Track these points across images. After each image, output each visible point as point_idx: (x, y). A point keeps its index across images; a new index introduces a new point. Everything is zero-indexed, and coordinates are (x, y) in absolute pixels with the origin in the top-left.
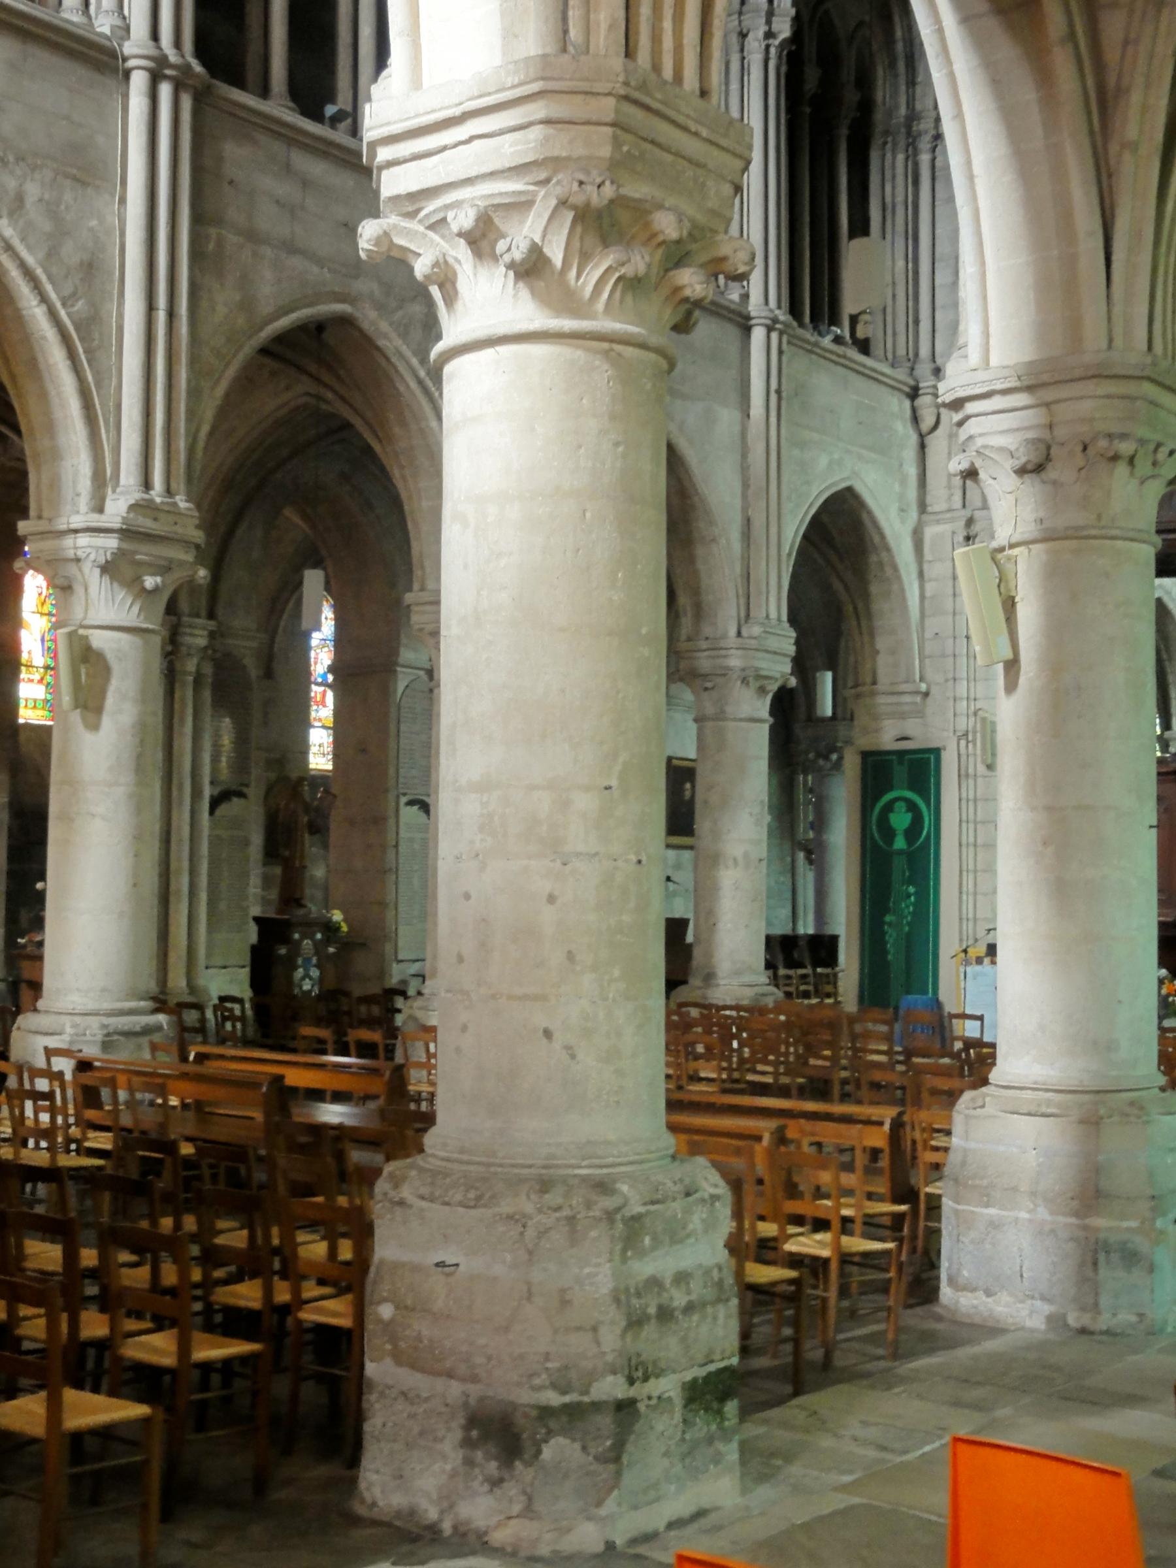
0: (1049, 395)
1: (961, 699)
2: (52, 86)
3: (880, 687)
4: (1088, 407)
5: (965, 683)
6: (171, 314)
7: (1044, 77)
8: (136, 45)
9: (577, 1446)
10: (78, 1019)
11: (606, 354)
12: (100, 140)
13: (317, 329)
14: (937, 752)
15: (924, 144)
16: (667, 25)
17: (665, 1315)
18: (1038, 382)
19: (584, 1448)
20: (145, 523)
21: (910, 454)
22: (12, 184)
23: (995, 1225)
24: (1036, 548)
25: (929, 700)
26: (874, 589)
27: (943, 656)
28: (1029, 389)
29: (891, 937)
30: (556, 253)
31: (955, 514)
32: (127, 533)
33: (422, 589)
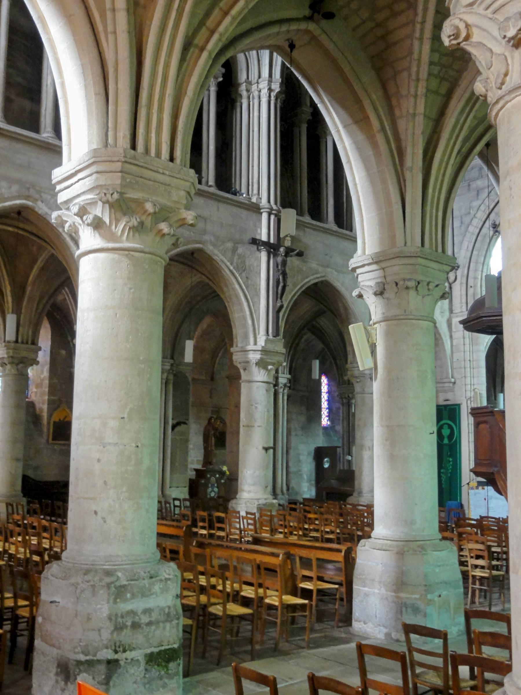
0: (383, 265)
1: (468, 384)
4: (398, 269)
5: (469, 378)
7: (374, 145)
9: (91, 677)
11: (127, 255)
13: (192, 253)
14: (459, 405)
16: (153, 135)
17: (135, 626)
18: (379, 260)
19: (94, 678)
23: (367, 595)
24: (382, 324)
25: (456, 385)
27: (461, 368)
28: (376, 263)
30: (107, 220)
31: (464, 313)
33: (237, 346)
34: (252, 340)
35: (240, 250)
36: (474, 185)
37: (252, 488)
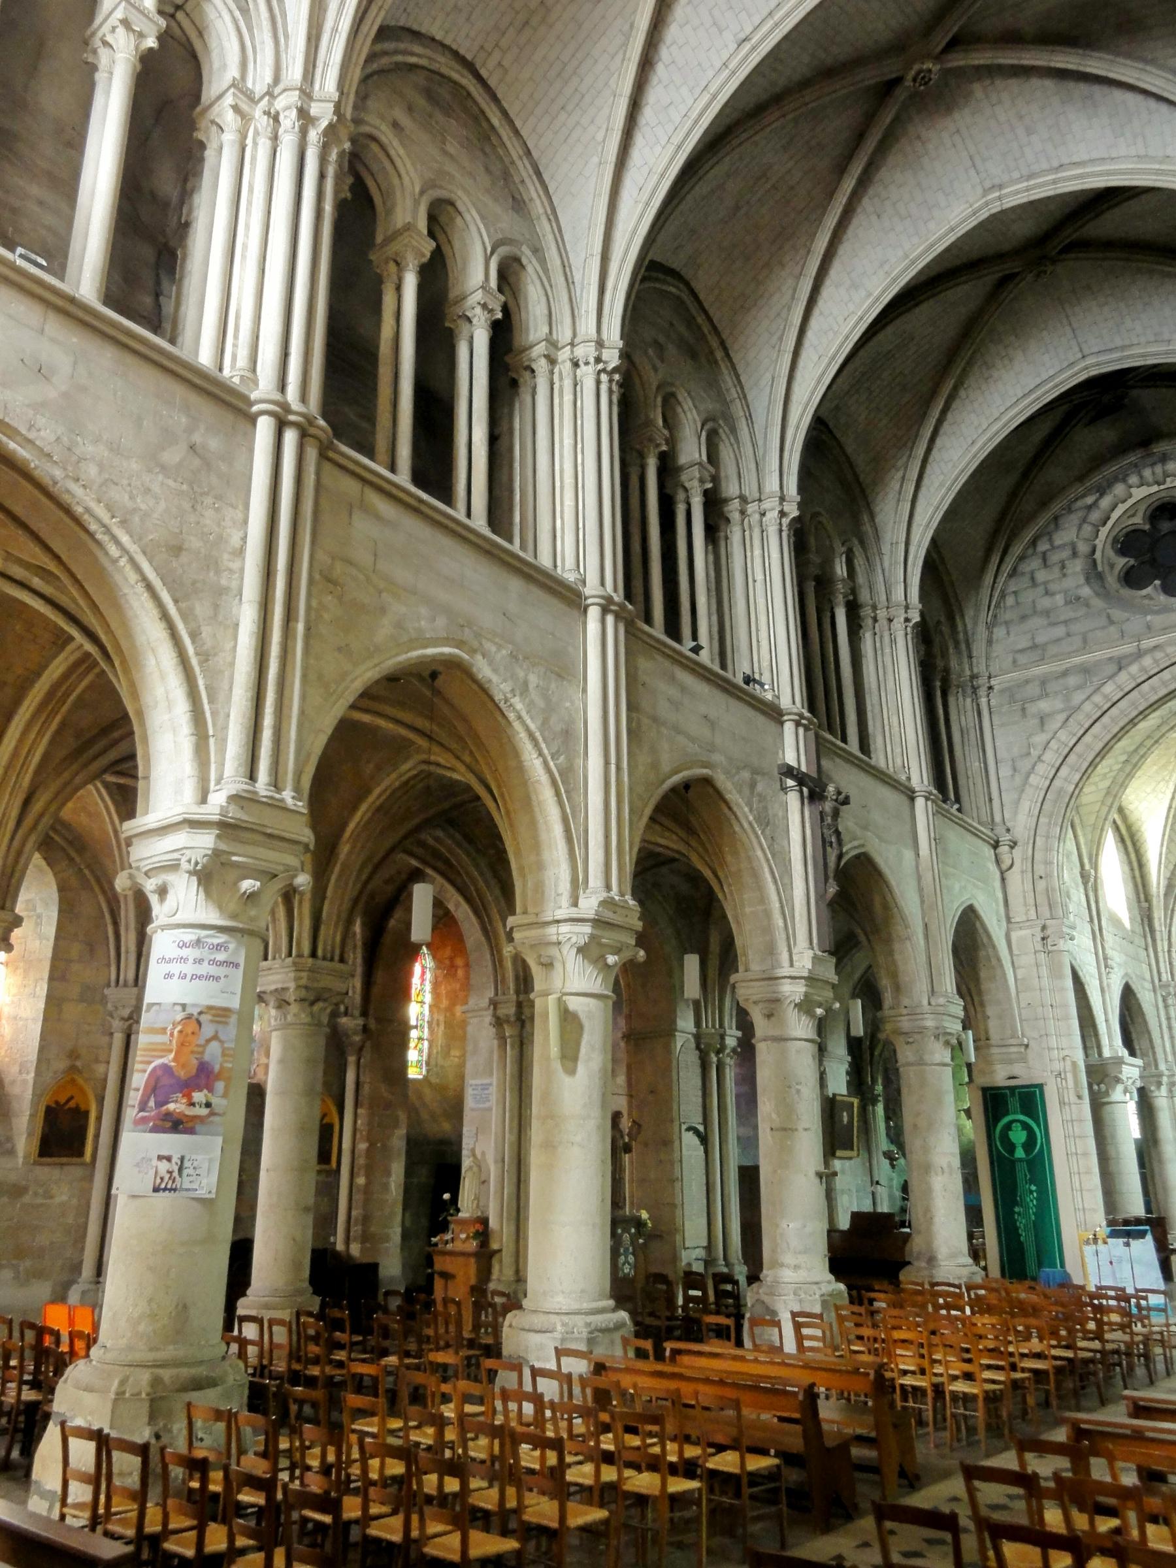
2: (543, 612)
3: (992, 1042)
6: (618, 768)
8: (591, 588)
10: (566, 1319)
12: (570, 649)
14: (1040, 1087)
15: (982, 692)
20: (608, 915)
21: (997, 884)
22: (521, 674)
26: (983, 974)
29: (1021, 1223)
32: (598, 922)
34: (785, 956)
35: (760, 788)
36: (1032, 709)
37: (802, 1259)
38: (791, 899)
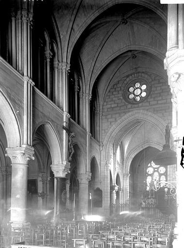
36: (109, 120)
38: (63, 151)
